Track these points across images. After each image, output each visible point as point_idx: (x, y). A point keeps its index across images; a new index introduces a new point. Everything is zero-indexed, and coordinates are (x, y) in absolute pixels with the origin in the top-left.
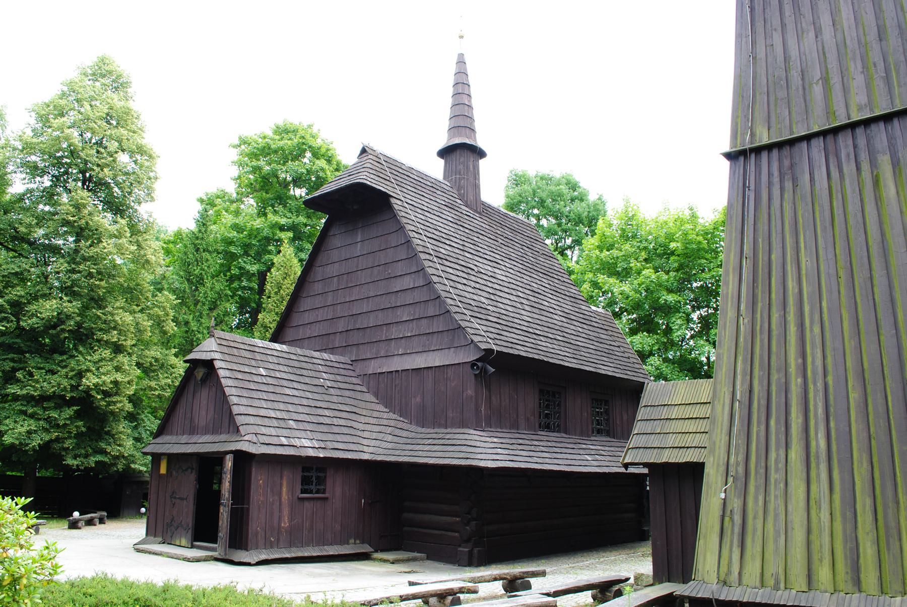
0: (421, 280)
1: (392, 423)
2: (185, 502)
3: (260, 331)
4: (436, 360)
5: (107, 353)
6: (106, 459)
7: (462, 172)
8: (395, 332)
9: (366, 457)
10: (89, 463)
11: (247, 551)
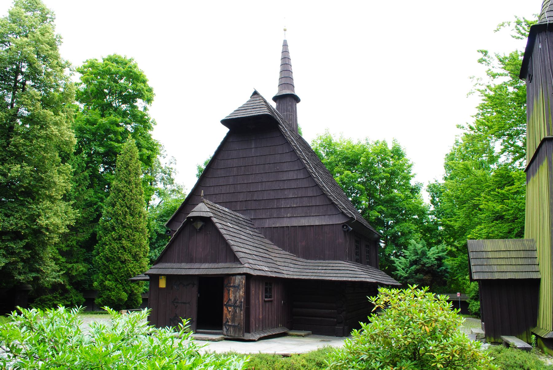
1: (289, 257)
2: (188, 305)
3: (115, 193)
4: (316, 221)
5: (48, 203)
6: (39, 275)
7: (290, 110)
8: (283, 204)
9: (286, 276)
10: (28, 278)
11: (249, 333)
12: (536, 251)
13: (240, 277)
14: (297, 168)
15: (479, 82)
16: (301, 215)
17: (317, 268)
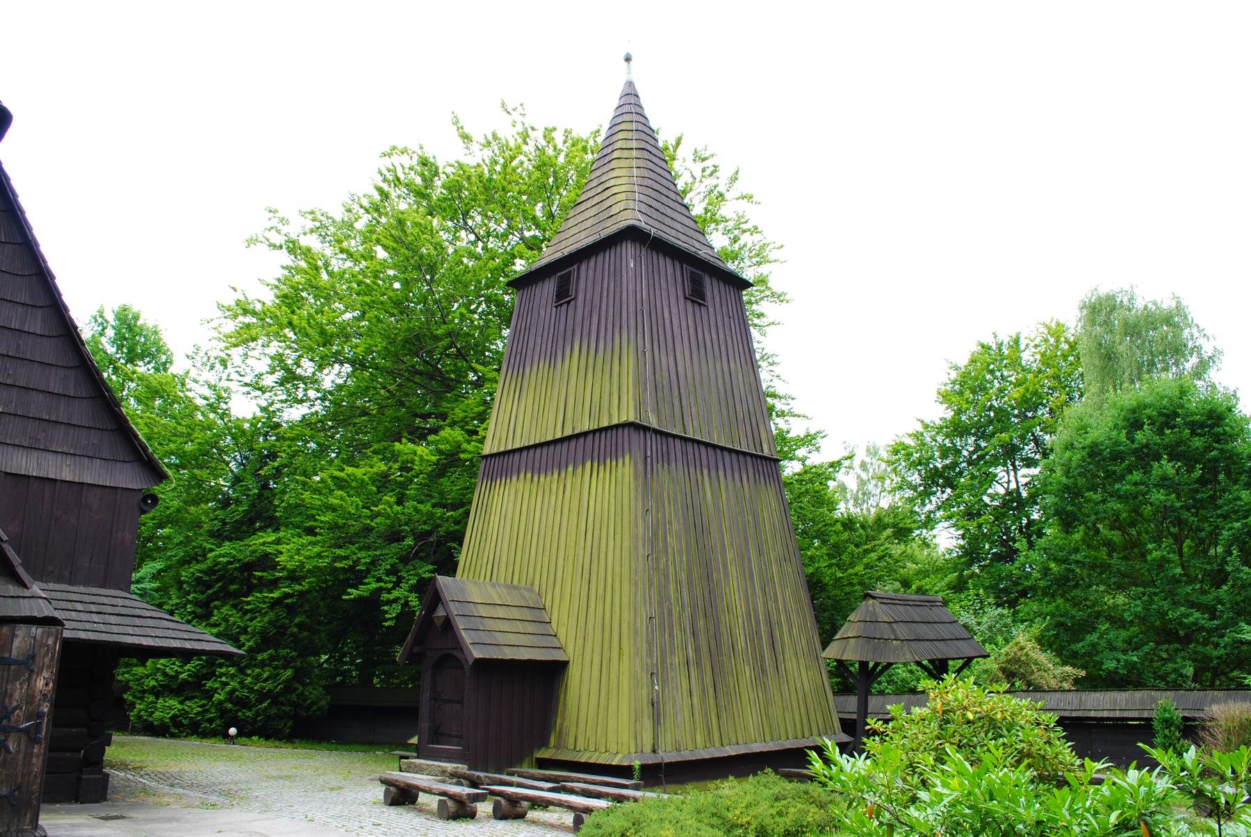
0: (39, 323)
4: (65, 471)
12: (543, 611)
13: (37, 631)
14: (24, 297)
15: (280, 226)
16: (16, 442)
17: (69, 606)
